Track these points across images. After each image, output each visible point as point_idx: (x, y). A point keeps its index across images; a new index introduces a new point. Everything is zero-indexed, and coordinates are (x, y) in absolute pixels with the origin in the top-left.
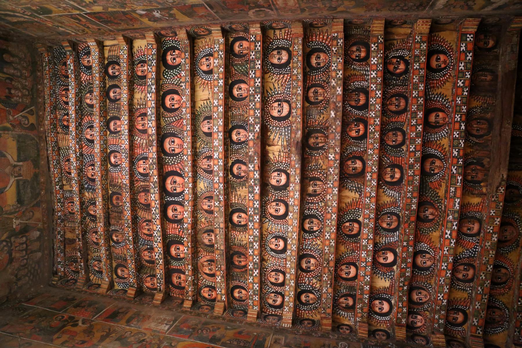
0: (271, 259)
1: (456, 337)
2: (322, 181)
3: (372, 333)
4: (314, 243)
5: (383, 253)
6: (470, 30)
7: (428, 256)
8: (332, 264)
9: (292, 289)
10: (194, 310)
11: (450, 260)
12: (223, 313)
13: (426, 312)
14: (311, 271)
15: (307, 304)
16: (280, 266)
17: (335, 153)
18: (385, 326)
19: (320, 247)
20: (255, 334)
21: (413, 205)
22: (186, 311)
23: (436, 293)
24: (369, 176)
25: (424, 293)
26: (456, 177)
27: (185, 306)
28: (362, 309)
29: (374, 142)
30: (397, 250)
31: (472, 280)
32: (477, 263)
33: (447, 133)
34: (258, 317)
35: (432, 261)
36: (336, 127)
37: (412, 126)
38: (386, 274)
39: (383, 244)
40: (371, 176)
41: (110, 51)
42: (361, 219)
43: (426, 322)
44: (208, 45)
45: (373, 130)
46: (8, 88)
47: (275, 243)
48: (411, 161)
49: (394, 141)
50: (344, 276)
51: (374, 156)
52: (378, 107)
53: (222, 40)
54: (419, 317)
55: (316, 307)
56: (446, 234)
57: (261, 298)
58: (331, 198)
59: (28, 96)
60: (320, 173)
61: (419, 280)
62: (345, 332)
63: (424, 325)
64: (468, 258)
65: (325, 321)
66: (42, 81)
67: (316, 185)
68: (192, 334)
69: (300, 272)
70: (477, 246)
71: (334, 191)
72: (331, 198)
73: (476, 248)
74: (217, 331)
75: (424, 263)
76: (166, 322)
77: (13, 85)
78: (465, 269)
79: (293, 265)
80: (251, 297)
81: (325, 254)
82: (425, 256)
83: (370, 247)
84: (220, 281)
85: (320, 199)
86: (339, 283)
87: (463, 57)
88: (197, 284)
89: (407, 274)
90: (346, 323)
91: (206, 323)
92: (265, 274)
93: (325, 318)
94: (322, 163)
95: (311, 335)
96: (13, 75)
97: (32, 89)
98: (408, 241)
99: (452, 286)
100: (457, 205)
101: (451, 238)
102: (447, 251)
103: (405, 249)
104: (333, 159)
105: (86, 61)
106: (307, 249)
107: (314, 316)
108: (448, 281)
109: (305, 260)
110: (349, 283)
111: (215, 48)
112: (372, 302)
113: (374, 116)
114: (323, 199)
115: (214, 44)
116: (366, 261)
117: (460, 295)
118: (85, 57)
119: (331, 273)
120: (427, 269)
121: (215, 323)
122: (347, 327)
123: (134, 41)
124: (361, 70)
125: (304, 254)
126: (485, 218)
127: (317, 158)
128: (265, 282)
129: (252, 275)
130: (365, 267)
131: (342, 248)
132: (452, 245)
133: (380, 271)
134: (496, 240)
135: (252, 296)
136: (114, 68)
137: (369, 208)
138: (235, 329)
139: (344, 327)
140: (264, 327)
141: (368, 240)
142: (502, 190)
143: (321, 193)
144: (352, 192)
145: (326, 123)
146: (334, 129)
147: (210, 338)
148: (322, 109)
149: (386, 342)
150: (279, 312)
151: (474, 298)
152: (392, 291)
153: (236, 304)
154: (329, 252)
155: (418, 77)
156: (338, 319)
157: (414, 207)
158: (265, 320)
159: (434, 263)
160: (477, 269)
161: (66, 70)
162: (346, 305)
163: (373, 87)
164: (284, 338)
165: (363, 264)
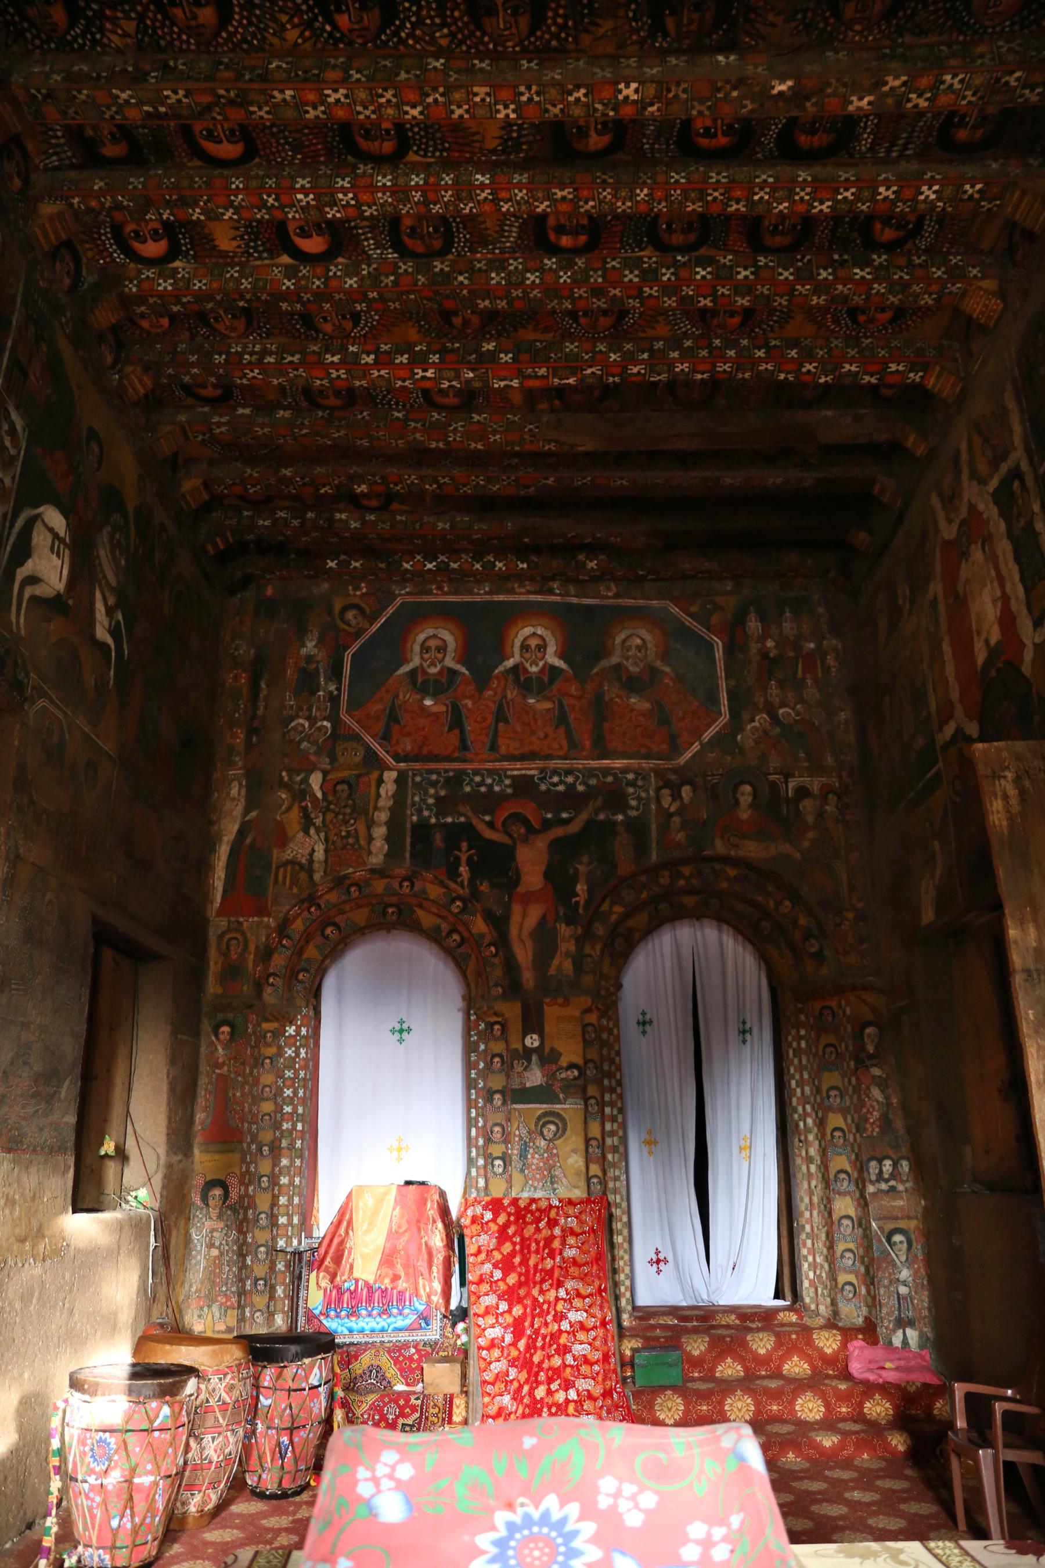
2: (532, 32)
4: (284, 18)
6: (933, 379)
13: (187, 335)
17: (642, 105)
18: (90, 254)
19: (275, 40)
21: (487, 302)
23: (258, 360)
24: (565, 193)
26: (573, 374)
28: (118, 207)
29: (672, 202)
33: (685, 333)
36: (736, 98)
37: (714, 287)
40: (564, 198)
42: (412, 157)
43: (158, 334)
45: (710, 198)
48: (617, 292)
49: (669, 226)
51: (629, 204)
52: (781, 207)
56: (425, 370)
58: (477, 99)
60: (563, 27)
67: (515, 14)
71: (506, 107)
72: (477, 99)
73: (397, 404)
75: (325, 319)
81: (263, 92)
85: (460, 30)
87: (872, 368)
89: (284, 306)
94: (602, 31)
100: (502, 384)
104: (621, 97)
113: (756, 198)
114: (461, 42)
116: (282, 207)
124: (913, 131)
126: (476, 418)
127: (621, 13)
130: (264, 204)
137: (461, 200)
142: (552, 446)
143: (484, 33)
144: (502, 128)
145: (748, 34)
146: (727, 95)
148: (805, 17)
154: (278, 105)
155: (846, 292)
157: (484, 304)
163: (848, 194)
165: (271, 200)
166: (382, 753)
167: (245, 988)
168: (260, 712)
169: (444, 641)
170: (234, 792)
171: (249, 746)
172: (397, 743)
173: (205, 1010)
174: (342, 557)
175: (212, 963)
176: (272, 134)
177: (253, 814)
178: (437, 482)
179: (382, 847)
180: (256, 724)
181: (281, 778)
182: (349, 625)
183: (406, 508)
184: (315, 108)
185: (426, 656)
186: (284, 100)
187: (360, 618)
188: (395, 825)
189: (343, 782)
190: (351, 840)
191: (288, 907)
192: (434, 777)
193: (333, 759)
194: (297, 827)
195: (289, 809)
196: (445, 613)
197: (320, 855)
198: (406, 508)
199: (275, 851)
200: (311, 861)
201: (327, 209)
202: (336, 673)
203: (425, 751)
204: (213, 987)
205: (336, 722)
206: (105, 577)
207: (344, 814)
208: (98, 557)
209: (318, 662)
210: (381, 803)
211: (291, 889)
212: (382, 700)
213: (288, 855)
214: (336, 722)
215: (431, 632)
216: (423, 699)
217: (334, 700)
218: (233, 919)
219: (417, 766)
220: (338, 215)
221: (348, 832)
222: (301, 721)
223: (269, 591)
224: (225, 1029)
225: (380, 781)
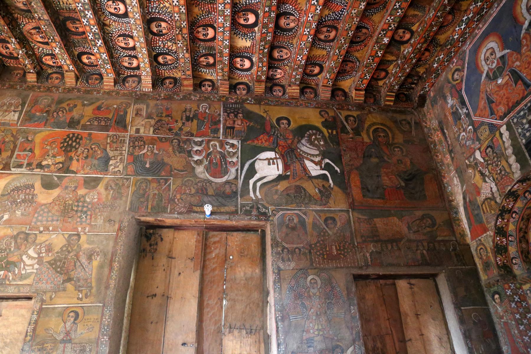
0: (114, 24)
1: (311, 84)
3: (233, 88)
4: (162, 5)
5: (244, 14)
7: (292, 17)
8: (185, 31)
9: (145, 56)
10: (41, 83)
11: (314, 26)
12: (77, 83)
14: (164, 35)
15: (165, 64)
16: (126, 31)
18: (246, 79)
19: (169, 10)
20: (115, 106)
22: (33, 86)
25: (285, 51)
27: (29, 80)
28: (222, 69)
30: (259, 11)
31: (333, 40)
32: (340, 26)
34: (116, 82)
35: (296, 23)
38: (247, 34)
39: (243, 4)
47: (114, 7)
50: (202, 37)
54: (279, 71)
55: (176, 67)
57: (113, 65)
61: (281, 40)
62: (207, 90)
63: (283, 76)
64: (333, 20)
65: (186, 83)
68: (47, 120)
69: (151, 36)
70: (344, 9)
73: (343, 11)
74: (74, 110)
75: (287, 24)
76: (13, 108)
78: (327, 30)
79: (141, 34)
80: (102, 66)
82: (288, 18)
83: (228, 12)
84: (59, 52)
86: (196, 44)
88: (34, 54)
89: (268, 39)
90: (209, 78)
91: (60, 102)
92: (111, 39)
93: (185, 79)
95: (173, 97)
98: (270, 7)
99: (313, 45)
101: (318, 4)
102: (312, 17)
103: (267, 14)
106: (155, 12)
107: (175, 74)
108: (308, 45)
109: (155, 23)
110: (209, 44)
112: (233, 59)
116: (223, 27)
117: (318, 52)
119: (185, 39)
120: (291, 30)
121: (70, 99)
122: (210, 83)
125: (151, 18)
128: (114, 48)
129: (95, 45)
131: (196, 10)
132: (317, 11)
133: (241, 32)
134: (363, 7)
135: (103, 65)
138: (93, 103)
139: (207, 83)
140: (124, 95)
141: (225, 4)
147: (68, 121)
149: (245, 97)
150: (137, 72)
151: (331, 57)
152: (253, 50)
153: (88, 69)
156: (200, 75)
158: (124, 84)
159: (298, 25)
160: (339, 32)
162: (207, 64)
164: (145, 106)
166: (495, 122)
167: (495, 271)
168: (449, 143)
169: (492, 48)
170: (455, 182)
171: (452, 159)
172: (498, 111)
173: (485, 289)
174: (436, 59)
175: (478, 265)
176: (204, 18)
177: (465, 187)
178: (397, 9)
179: (517, 168)
180: (450, 148)
181: (466, 163)
182: (457, 80)
183: (417, 24)
184: (181, 9)
185: (488, 62)
186: (179, 17)
187: (459, 73)
188: (517, 152)
189: (488, 147)
190: (503, 173)
191: (493, 223)
192: (522, 113)
193: (479, 140)
194: (481, 181)
195: (475, 175)
196: (485, 36)
197: (495, 189)
198: (417, 24)
199: (478, 198)
200: (493, 194)
201: (226, 14)
202: (463, 103)
203: (511, 105)
204: (483, 277)
205: (472, 123)
206: (308, 154)
207: (495, 162)
208: (301, 150)
209: (455, 105)
210: (507, 145)
211: (491, 212)
212: (482, 98)
213: (483, 197)
214: (472, 123)
215: (485, 50)
216: (497, 81)
217: (468, 115)
218: (477, 239)
219: (512, 114)
220: (229, 11)
221: (500, 169)
222: (462, 134)
223: (432, 94)
224: (497, 296)
225: (501, 135)
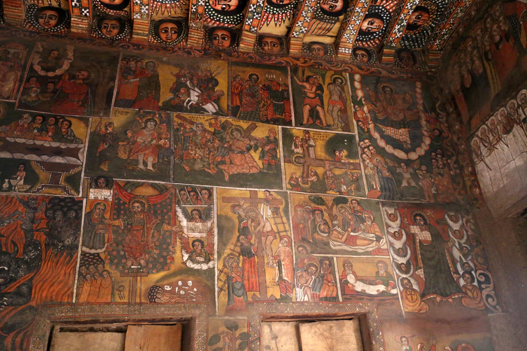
41: (329, 30)
44: (166, 7)
46: (497, 48)
53: (137, 16)
59: (491, 15)
66: (466, 18)
77: (490, 46)
96: (480, 58)
97: (481, 19)
105: (375, 24)
111: (147, 9)
115: (148, 14)
118: (376, 30)
123: (284, 34)
136: (331, 7)
161: (419, 18)
